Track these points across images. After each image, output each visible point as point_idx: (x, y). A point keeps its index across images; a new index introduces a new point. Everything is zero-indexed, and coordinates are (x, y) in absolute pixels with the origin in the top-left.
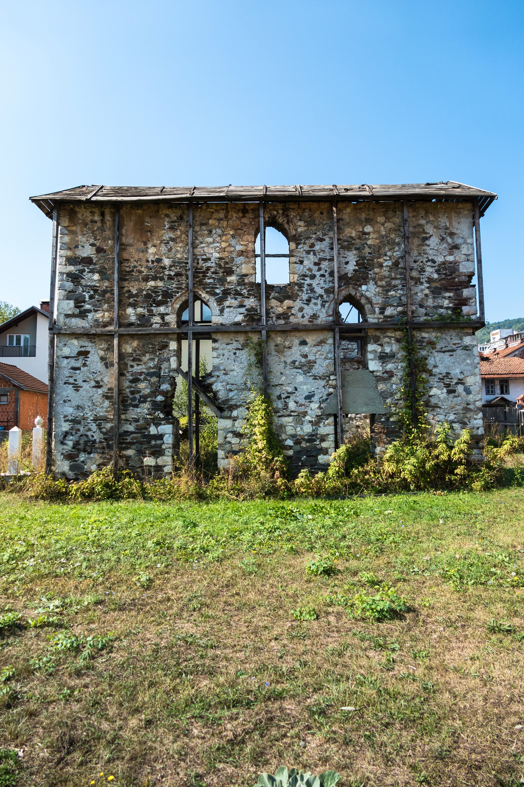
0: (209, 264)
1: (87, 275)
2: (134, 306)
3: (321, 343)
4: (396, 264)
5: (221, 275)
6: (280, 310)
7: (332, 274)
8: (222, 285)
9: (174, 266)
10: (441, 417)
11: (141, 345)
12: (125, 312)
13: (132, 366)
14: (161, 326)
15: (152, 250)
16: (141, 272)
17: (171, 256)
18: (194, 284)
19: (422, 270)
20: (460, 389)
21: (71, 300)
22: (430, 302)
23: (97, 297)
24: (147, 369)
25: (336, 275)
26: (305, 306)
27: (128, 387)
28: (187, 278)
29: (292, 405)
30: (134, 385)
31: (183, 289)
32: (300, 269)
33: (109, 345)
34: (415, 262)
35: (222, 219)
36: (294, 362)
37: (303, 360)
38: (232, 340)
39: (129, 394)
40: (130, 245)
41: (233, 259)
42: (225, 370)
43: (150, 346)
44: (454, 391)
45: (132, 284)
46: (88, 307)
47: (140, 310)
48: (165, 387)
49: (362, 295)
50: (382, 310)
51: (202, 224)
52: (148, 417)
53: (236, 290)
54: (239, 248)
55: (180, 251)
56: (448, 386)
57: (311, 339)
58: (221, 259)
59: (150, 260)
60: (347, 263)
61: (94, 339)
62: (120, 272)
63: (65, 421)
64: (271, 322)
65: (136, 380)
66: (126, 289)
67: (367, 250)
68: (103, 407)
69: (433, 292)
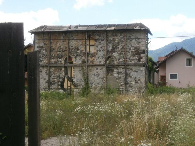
0: (73, 47)
2: (53, 59)
3: (102, 69)
4: (123, 47)
6: (91, 60)
7: (105, 50)
8: (76, 53)
10: (133, 89)
13: (53, 75)
15: (58, 44)
19: (130, 49)
20: (139, 82)
22: (132, 58)
25: (106, 50)
26: (98, 59)
29: (94, 85)
32: (96, 48)
34: (128, 47)
35: (76, 35)
36: (94, 74)
37: (97, 74)
44: (137, 83)
46: (42, 59)
47: (55, 60)
48: (61, 80)
49: (113, 56)
50: (119, 60)
51: (71, 37)
54: (81, 43)
56: (136, 81)
57: (99, 68)
58: (76, 46)
60: (109, 47)
62: (50, 50)
64: (88, 63)
65: (54, 78)
67: (115, 44)
69: (133, 55)
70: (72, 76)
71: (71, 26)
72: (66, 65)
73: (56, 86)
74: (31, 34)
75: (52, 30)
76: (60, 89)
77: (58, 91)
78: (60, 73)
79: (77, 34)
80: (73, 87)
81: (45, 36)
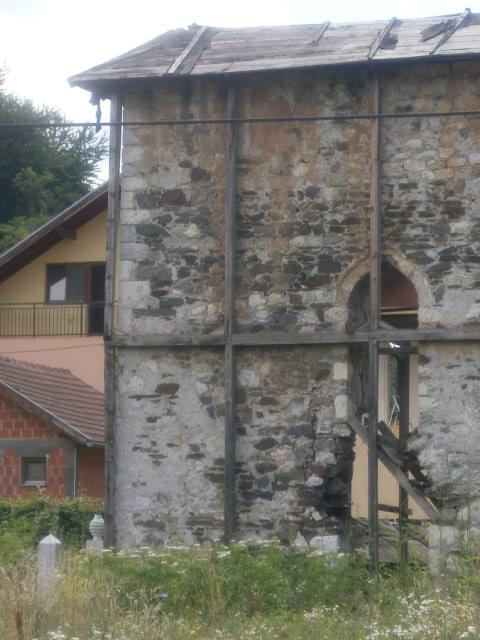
1: (174, 228)
2: (264, 289)
5: (438, 217)
8: (441, 239)
9: (343, 202)
11: (277, 369)
12: (247, 304)
13: (260, 415)
14: (316, 330)
15: (300, 170)
16: (276, 218)
17: (337, 182)
18: (382, 240)
21: (143, 279)
23: (193, 271)
24: (290, 420)
27: (252, 458)
28: (369, 228)
30: (263, 452)
31: (363, 251)
33: (217, 371)
35: (439, 98)
38: (458, 358)
39: (254, 472)
40: (258, 162)
41: (462, 185)
42: (444, 423)
43: (296, 373)
45: (260, 244)
46: (175, 293)
47: (275, 298)
48: (325, 457)
52: (291, 518)
53: (469, 251)
55: (358, 170)
58: (438, 183)
59: (295, 190)
61: (188, 358)
62: (238, 218)
63: (136, 524)
65: (267, 444)
66: (249, 254)
68: (205, 498)
70: (414, 421)
71: (396, 23)
72: (361, 336)
73: (284, 502)
74: (95, 101)
75: (272, 56)
76: (315, 524)
77: (299, 542)
78: (316, 404)
79: (442, 87)
80: (417, 509)
81: (194, 109)
